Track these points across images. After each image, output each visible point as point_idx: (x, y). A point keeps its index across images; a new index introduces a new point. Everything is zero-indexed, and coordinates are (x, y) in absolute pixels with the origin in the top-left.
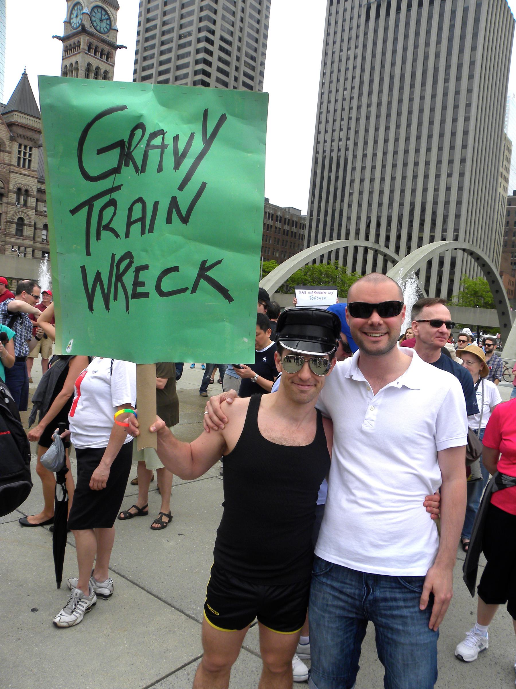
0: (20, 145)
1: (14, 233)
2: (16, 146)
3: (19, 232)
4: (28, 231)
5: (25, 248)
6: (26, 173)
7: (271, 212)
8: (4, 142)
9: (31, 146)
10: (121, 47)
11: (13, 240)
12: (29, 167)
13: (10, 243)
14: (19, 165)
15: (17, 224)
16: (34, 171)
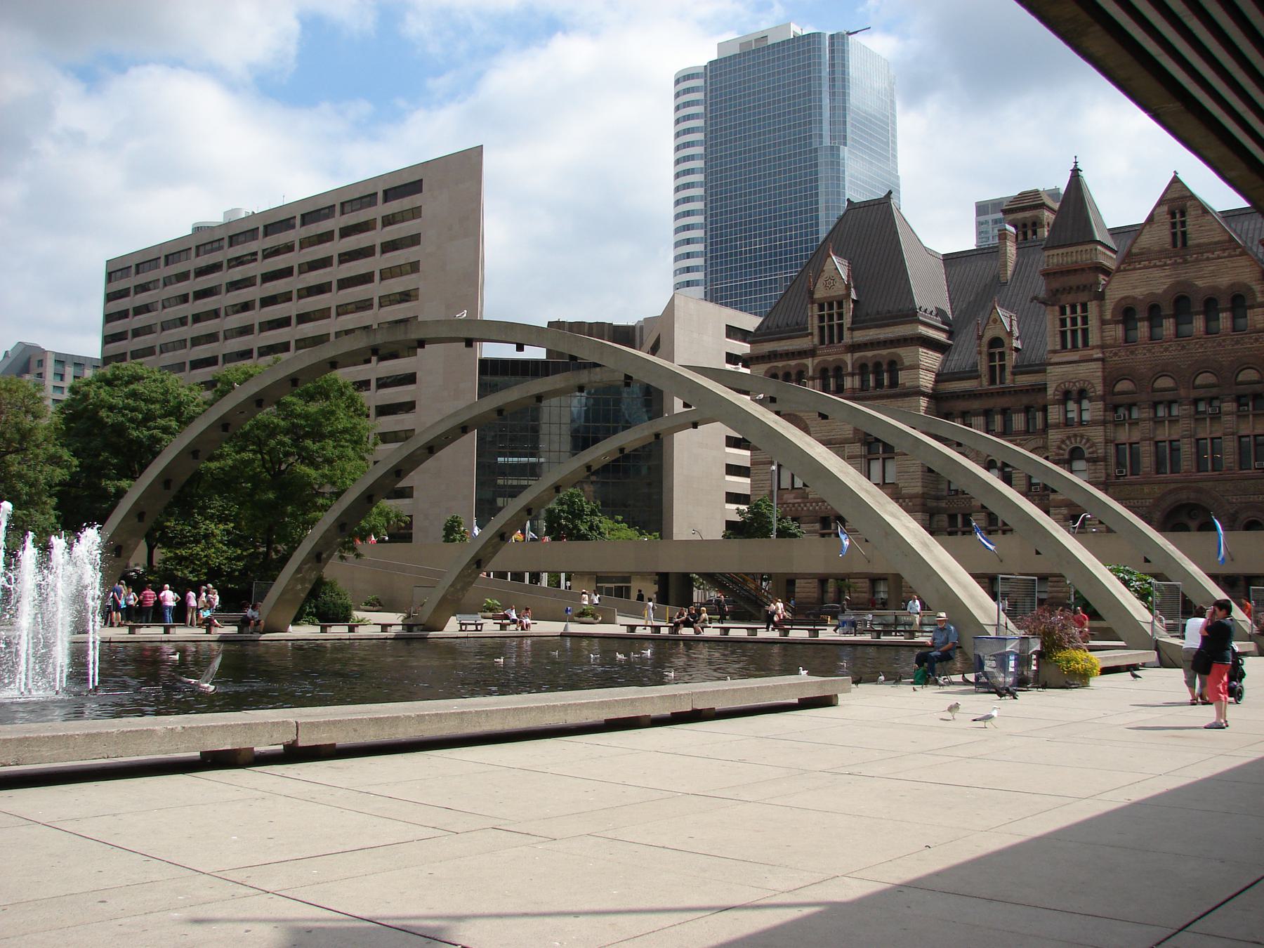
8: (1250, 289)
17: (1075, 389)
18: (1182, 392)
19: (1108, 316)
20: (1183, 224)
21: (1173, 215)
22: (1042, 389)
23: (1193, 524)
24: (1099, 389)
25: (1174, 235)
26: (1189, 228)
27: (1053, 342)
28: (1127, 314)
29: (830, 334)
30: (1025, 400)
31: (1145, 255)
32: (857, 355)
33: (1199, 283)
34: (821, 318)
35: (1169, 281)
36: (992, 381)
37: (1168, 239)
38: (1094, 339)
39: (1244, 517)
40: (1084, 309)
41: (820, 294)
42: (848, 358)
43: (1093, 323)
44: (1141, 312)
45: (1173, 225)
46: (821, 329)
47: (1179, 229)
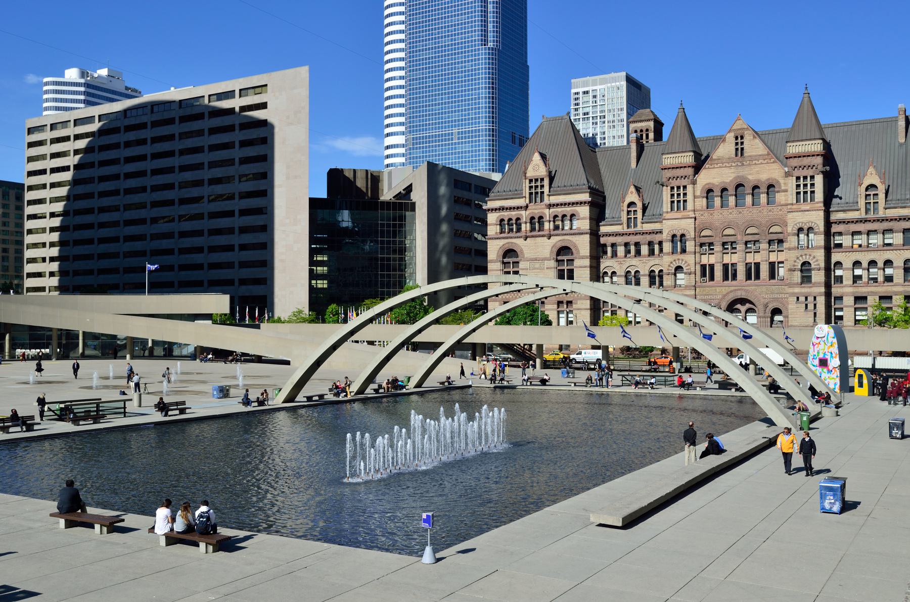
0: (798, 178)
1: (799, 281)
3: (806, 279)
5: (815, 298)
6: (808, 208)
8: (778, 182)
9: (812, 174)
11: (797, 290)
12: (812, 199)
13: (792, 294)
14: (798, 201)
15: (801, 271)
16: (818, 203)
17: (678, 234)
18: (739, 237)
19: (698, 193)
20: (742, 143)
21: (737, 138)
23: (743, 309)
24: (692, 234)
25: (737, 149)
26: (745, 146)
27: (666, 206)
29: (536, 195)
30: (649, 238)
32: (552, 210)
33: (750, 177)
34: (531, 187)
35: (733, 176)
36: (628, 227)
37: (734, 152)
38: (690, 205)
39: (771, 306)
40: (685, 187)
41: (530, 173)
42: (547, 211)
43: (689, 197)
44: (717, 192)
45: (737, 144)
46: (531, 194)
47: (739, 147)
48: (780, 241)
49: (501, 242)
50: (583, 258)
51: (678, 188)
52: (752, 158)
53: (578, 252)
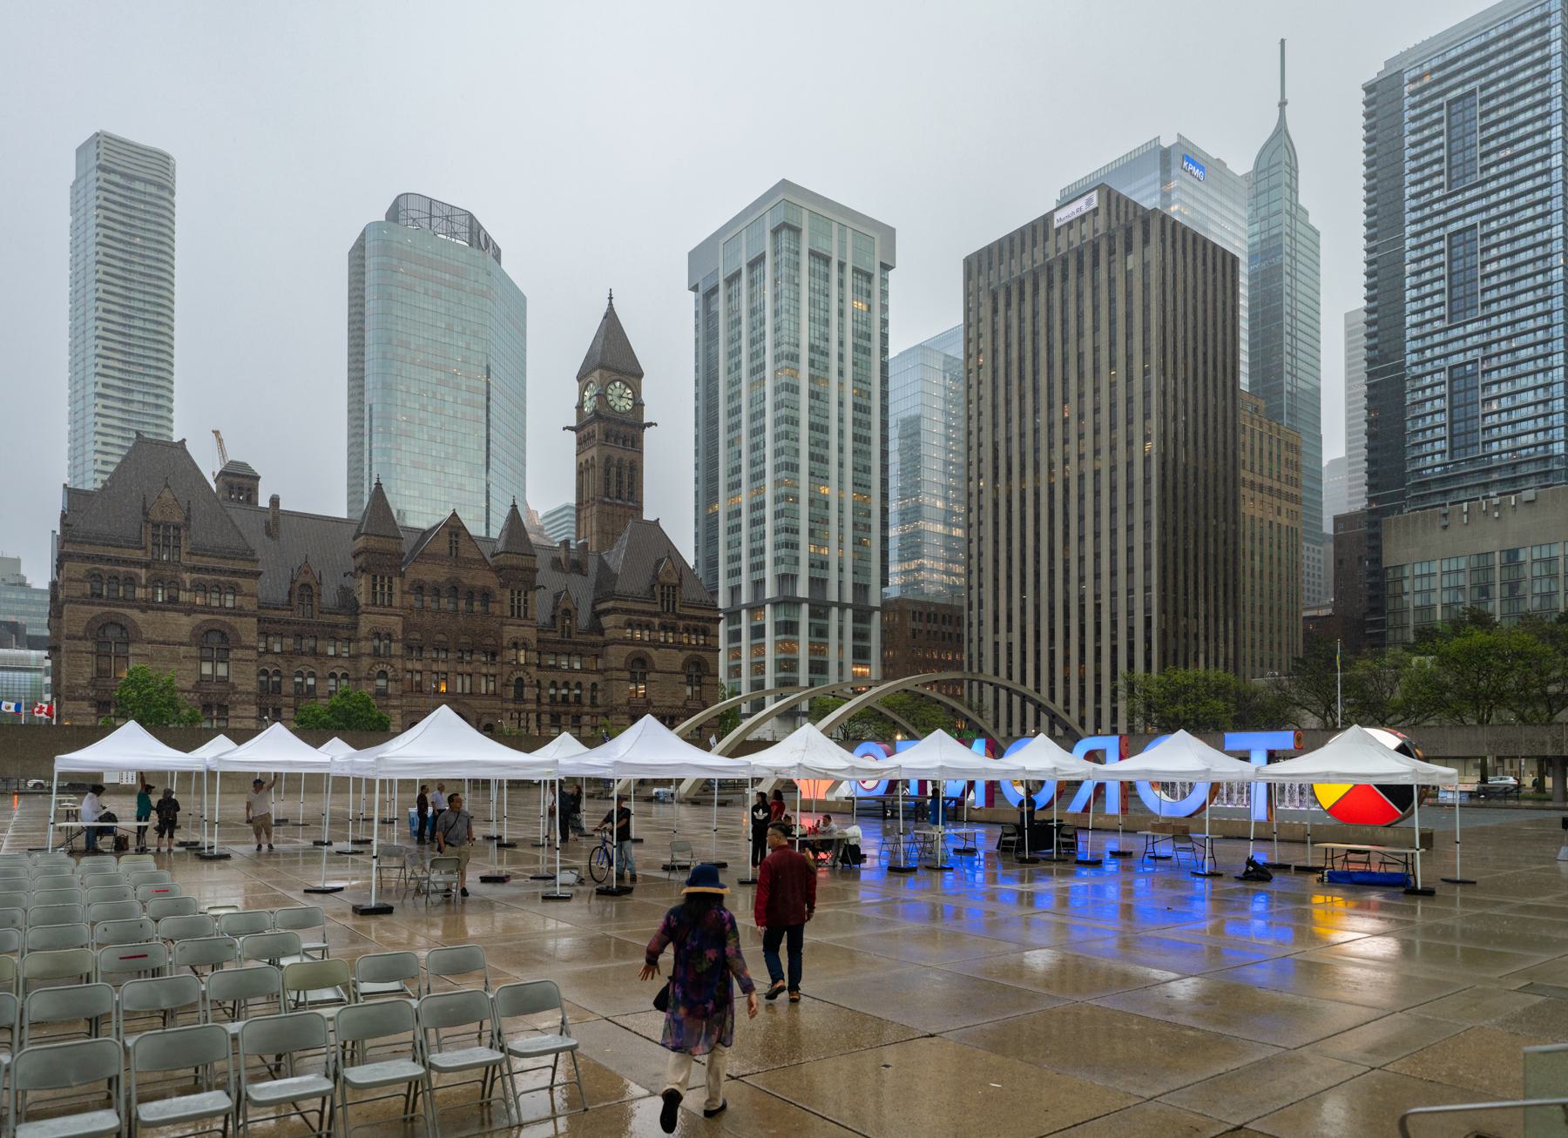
2: (508, 593)
3: (519, 697)
4: (529, 693)
7: (919, 609)
10: (650, 425)
19: (406, 588)
21: (450, 534)
22: (355, 626)
28: (419, 588)
31: (433, 556)
32: (195, 576)
38: (396, 601)
48: (494, 655)
49: (98, 610)
50: (243, 647)
51: (382, 578)
52: (469, 561)
53: (239, 639)
